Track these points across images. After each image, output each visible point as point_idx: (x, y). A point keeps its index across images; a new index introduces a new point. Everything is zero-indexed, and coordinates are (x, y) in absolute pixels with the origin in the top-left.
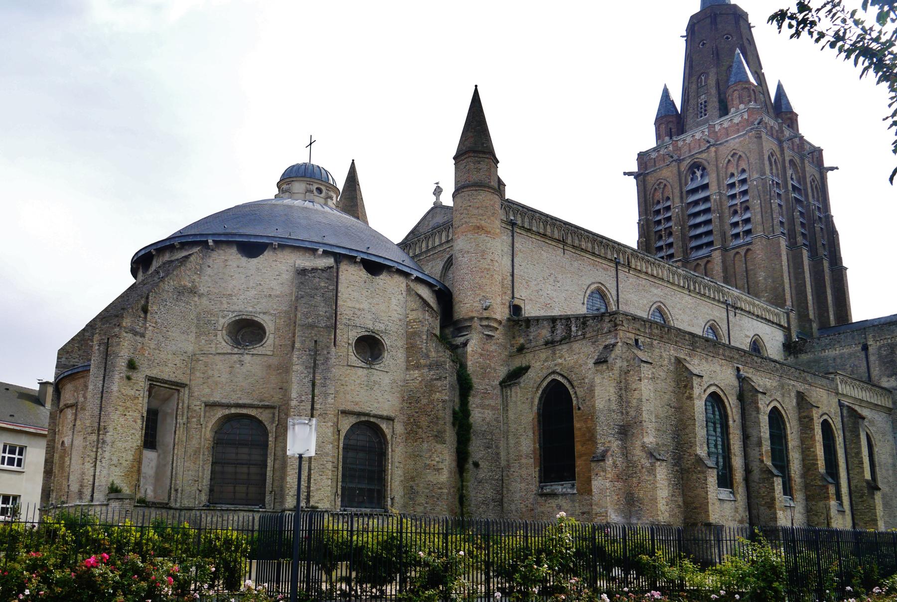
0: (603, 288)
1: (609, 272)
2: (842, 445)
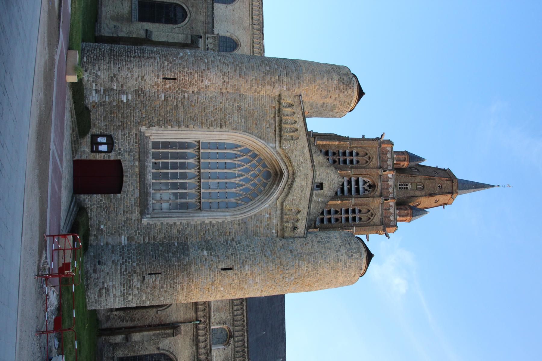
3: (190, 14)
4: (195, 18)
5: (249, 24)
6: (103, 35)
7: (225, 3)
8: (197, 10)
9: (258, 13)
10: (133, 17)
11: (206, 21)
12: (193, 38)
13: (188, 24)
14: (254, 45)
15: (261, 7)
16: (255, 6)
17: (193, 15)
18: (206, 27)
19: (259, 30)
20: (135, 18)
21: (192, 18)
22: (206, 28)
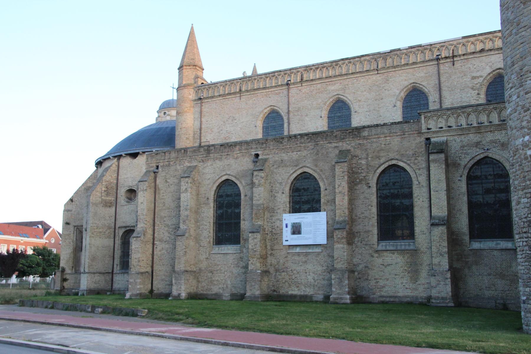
0: (275, 108)
1: (281, 95)
2: (424, 183)
3: (392, 159)
4: (397, 151)
5: (378, 75)
6: (450, 294)
7: (350, 115)
8: (383, 150)
9: (358, 63)
10: (407, 248)
11: (399, 134)
12: (435, 151)
13: (408, 162)
14: (411, 62)
15: (349, 61)
16: (348, 70)
17: (391, 155)
18: (410, 133)
19: (385, 59)
20: (409, 245)
21: (397, 157)
22: (412, 133)
